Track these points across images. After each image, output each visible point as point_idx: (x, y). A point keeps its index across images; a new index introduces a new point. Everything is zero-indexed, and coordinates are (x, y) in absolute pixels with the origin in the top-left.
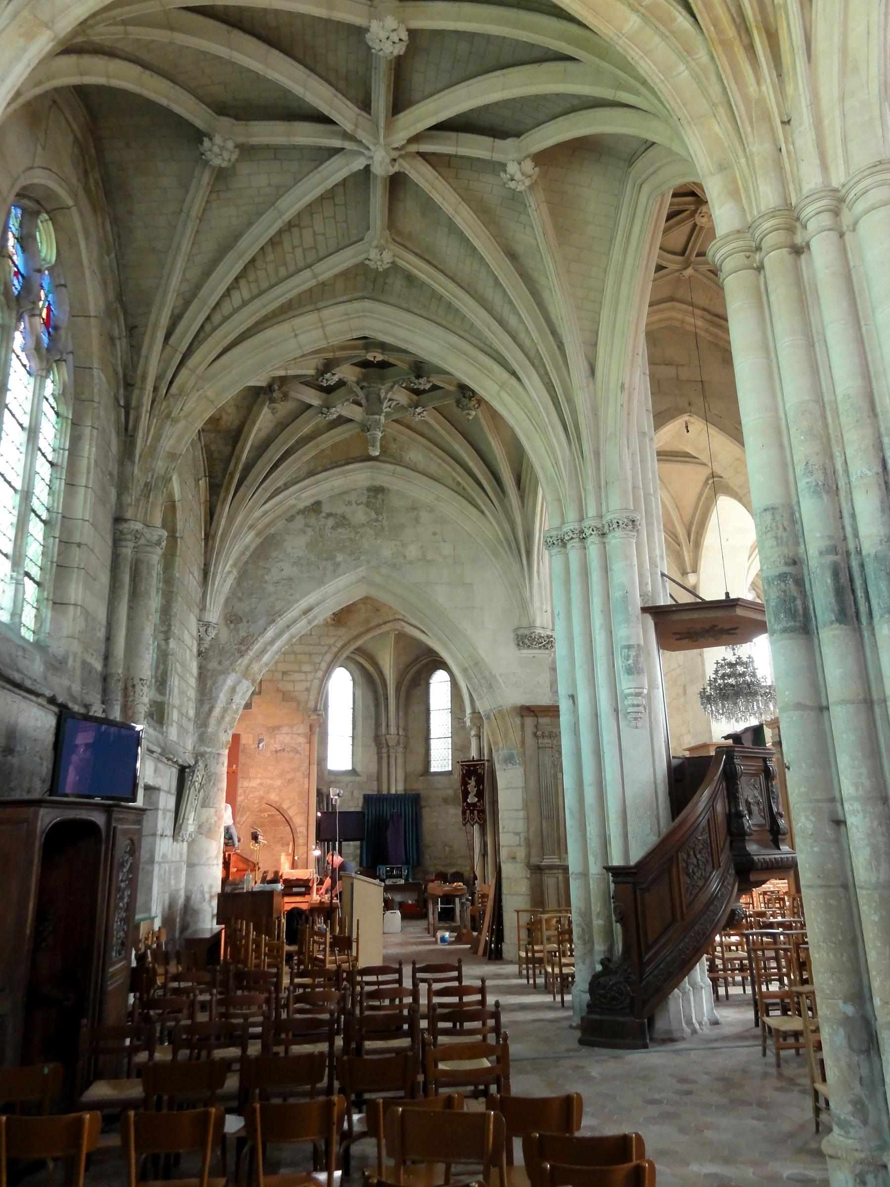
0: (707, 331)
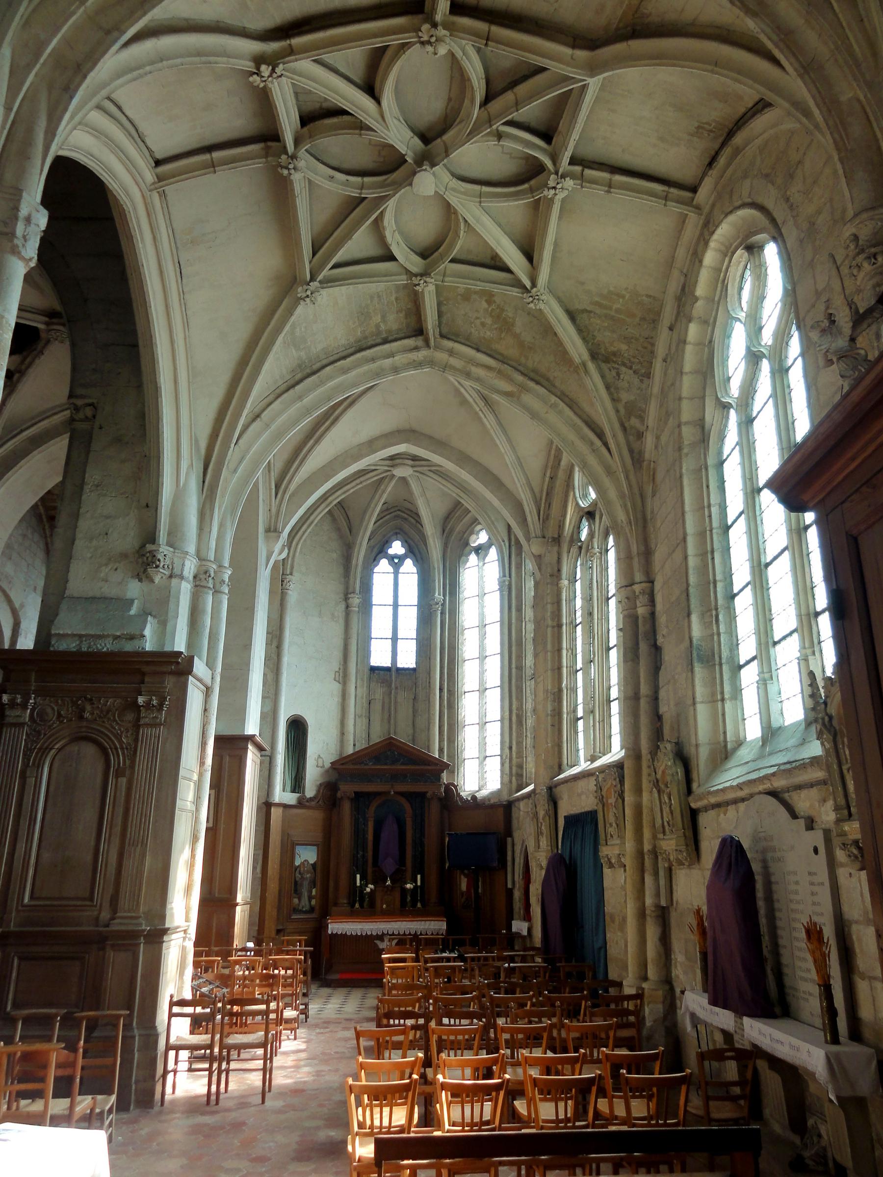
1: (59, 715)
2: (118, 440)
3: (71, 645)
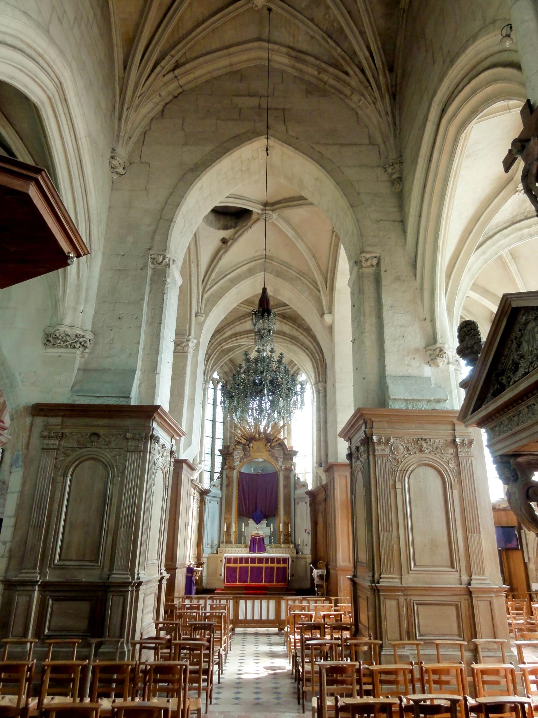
0: (293, 67)
1: (408, 449)
2: (398, 279)
3: (401, 406)
